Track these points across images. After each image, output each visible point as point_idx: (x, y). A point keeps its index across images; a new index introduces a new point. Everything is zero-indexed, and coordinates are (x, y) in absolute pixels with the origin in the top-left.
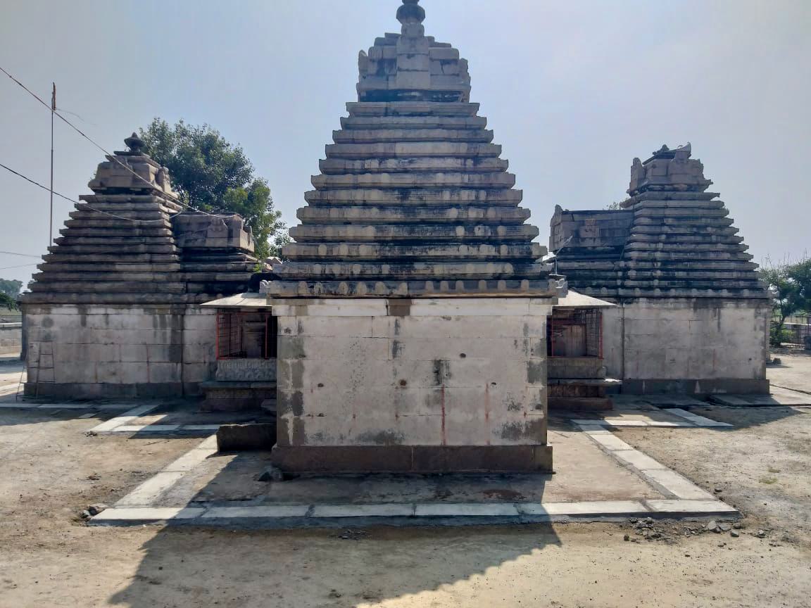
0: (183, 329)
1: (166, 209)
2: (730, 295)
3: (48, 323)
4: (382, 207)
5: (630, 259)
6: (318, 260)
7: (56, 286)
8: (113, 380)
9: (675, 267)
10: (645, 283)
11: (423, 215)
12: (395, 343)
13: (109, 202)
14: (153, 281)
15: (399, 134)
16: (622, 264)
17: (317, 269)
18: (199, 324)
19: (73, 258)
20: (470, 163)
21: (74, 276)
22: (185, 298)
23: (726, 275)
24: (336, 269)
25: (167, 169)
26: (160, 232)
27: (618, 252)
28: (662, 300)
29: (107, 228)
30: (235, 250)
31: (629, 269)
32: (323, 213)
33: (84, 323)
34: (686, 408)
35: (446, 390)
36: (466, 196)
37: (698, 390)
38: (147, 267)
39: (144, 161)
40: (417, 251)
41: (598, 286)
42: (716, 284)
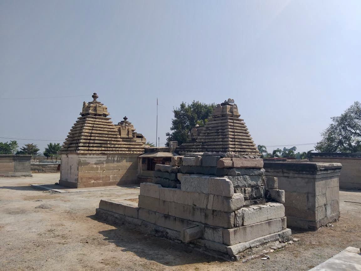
23: (218, 147)
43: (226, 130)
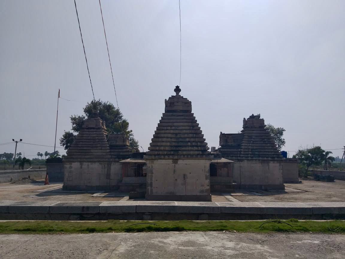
0: (110, 169)
1: (105, 133)
2: (271, 159)
3: (71, 167)
4: (171, 138)
5: (242, 148)
6: (157, 150)
7: (74, 156)
8: (89, 185)
9: (255, 151)
10: (246, 155)
11: (181, 140)
12: (174, 170)
13: (88, 132)
14: (102, 155)
15: (175, 121)
16: (240, 150)
17: (156, 153)
18: (115, 168)
19: (79, 148)
20: (192, 128)
21: (79, 154)
22: (111, 160)
23: (270, 153)
24: (161, 153)
25: (105, 122)
26: (104, 141)
27: (239, 146)
28: (251, 161)
29: (88, 139)
30: (125, 145)
31: (242, 151)
32: (157, 139)
33: (81, 167)
34: (257, 192)
35: (186, 181)
36: (191, 135)
37: (263, 188)
38: (100, 151)
39: (99, 119)
40: (179, 148)
41: (233, 157)
42: (267, 156)
43: (271, 140)
